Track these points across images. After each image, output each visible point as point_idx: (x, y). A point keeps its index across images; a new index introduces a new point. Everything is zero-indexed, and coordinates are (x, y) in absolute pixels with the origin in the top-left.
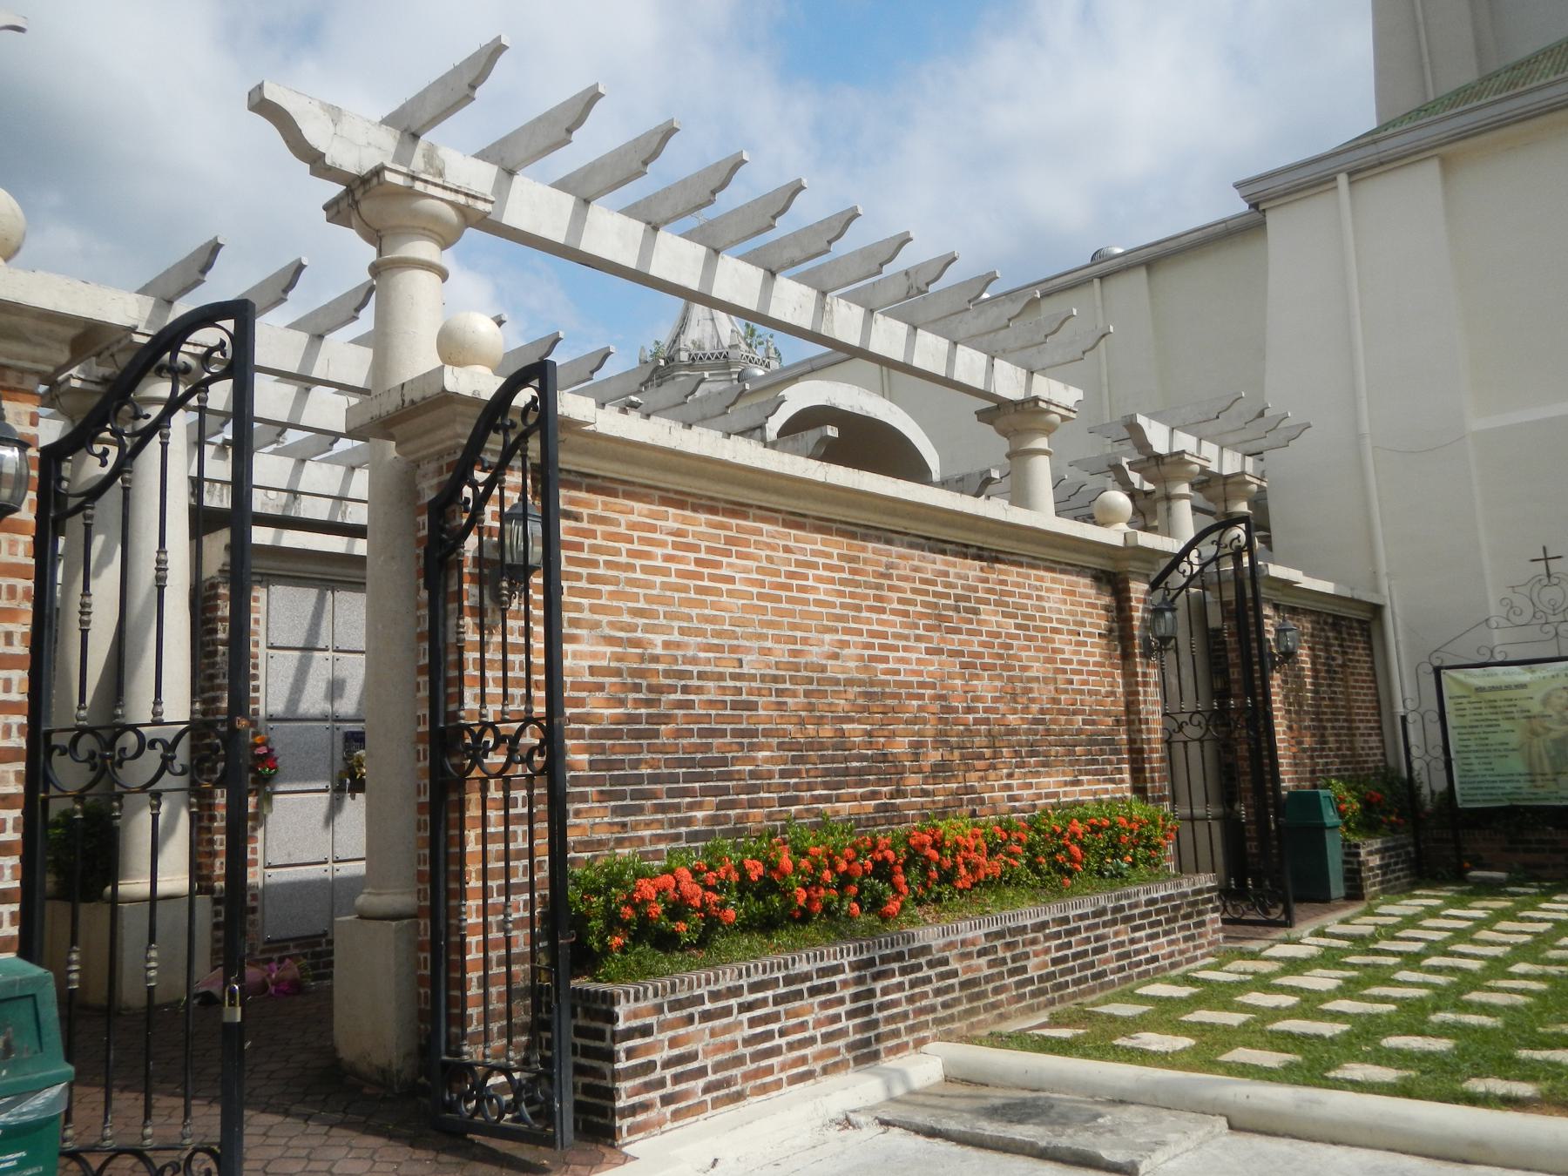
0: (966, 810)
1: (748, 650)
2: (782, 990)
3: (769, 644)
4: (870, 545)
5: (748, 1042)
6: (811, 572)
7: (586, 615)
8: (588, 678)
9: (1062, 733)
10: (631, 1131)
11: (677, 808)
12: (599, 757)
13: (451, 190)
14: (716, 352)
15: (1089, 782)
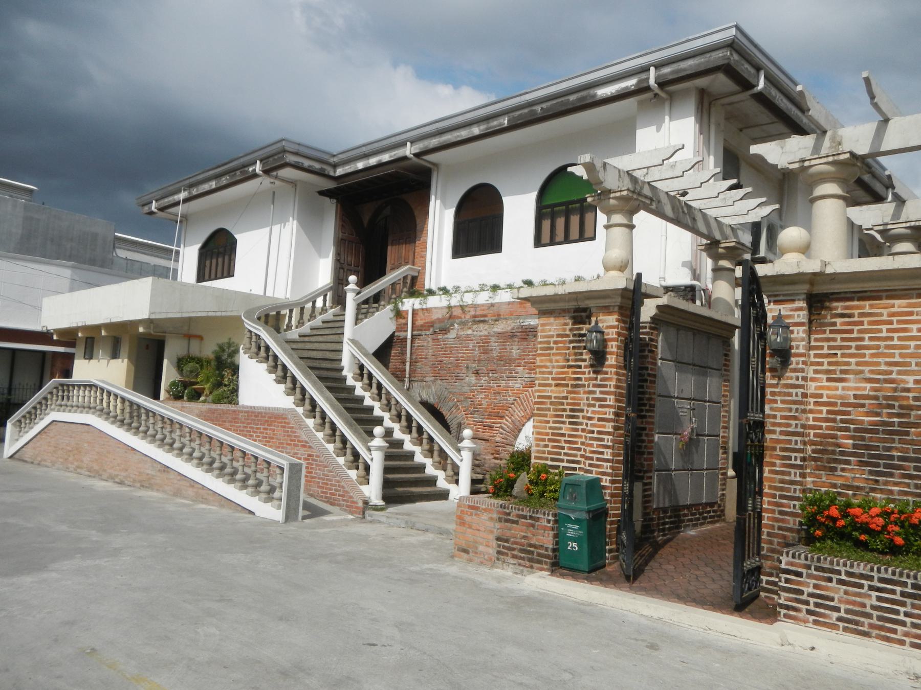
2: (909, 590)
7: (853, 367)
8: (852, 401)
10: (785, 616)
12: (860, 442)
13: (824, 157)
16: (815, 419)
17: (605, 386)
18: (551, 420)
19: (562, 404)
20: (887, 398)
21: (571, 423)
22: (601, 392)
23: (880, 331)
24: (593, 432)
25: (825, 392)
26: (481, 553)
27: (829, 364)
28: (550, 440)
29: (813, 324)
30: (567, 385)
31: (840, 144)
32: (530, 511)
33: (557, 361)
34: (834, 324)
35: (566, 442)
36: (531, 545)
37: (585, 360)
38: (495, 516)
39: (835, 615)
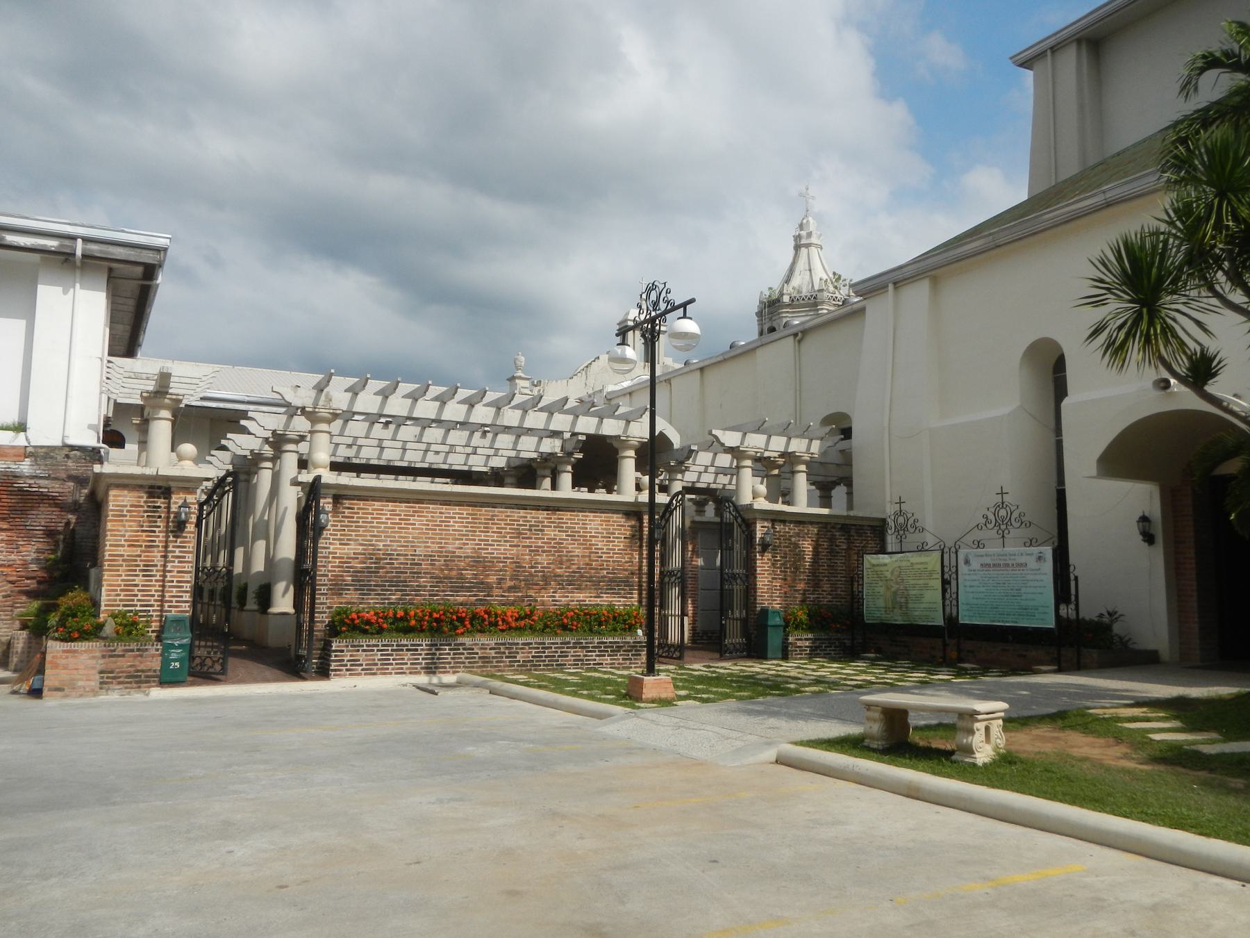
0: (525, 603)
1: (419, 547)
2: (395, 648)
3: (429, 544)
4: (484, 509)
5: (379, 660)
6: (452, 520)
7: (354, 537)
9: (591, 577)
10: (334, 675)
11: (385, 595)
14: (809, 295)
15: (607, 597)
16: (332, 567)
17: (185, 547)
18: (123, 574)
19: (136, 561)
20: (370, 554)
21: (144, 576)
22: (180, 552)
23: (368, 518)
24: (173, 581)
25: (338, 551)
26: (80, 687)
27: (341, 535)
28: (122, 590)
29: (335, 511)
30: (141, 546)
31: (331, 400)
32: (137, 645)
33: (130, 526)
34: (344, 513)
35: (139, 590)
36: (138, 671)
37: (159, 527)
38: (98, 654)
39: (361, 668)
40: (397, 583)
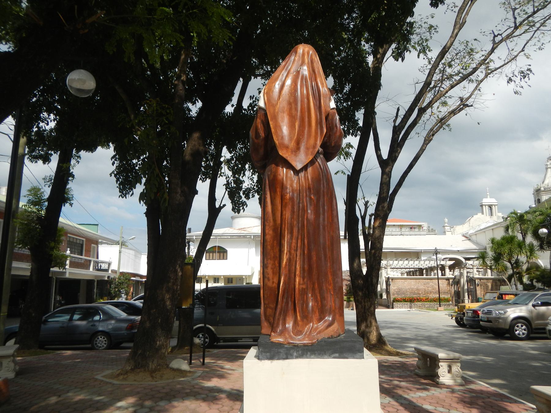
40: (404, 293)
